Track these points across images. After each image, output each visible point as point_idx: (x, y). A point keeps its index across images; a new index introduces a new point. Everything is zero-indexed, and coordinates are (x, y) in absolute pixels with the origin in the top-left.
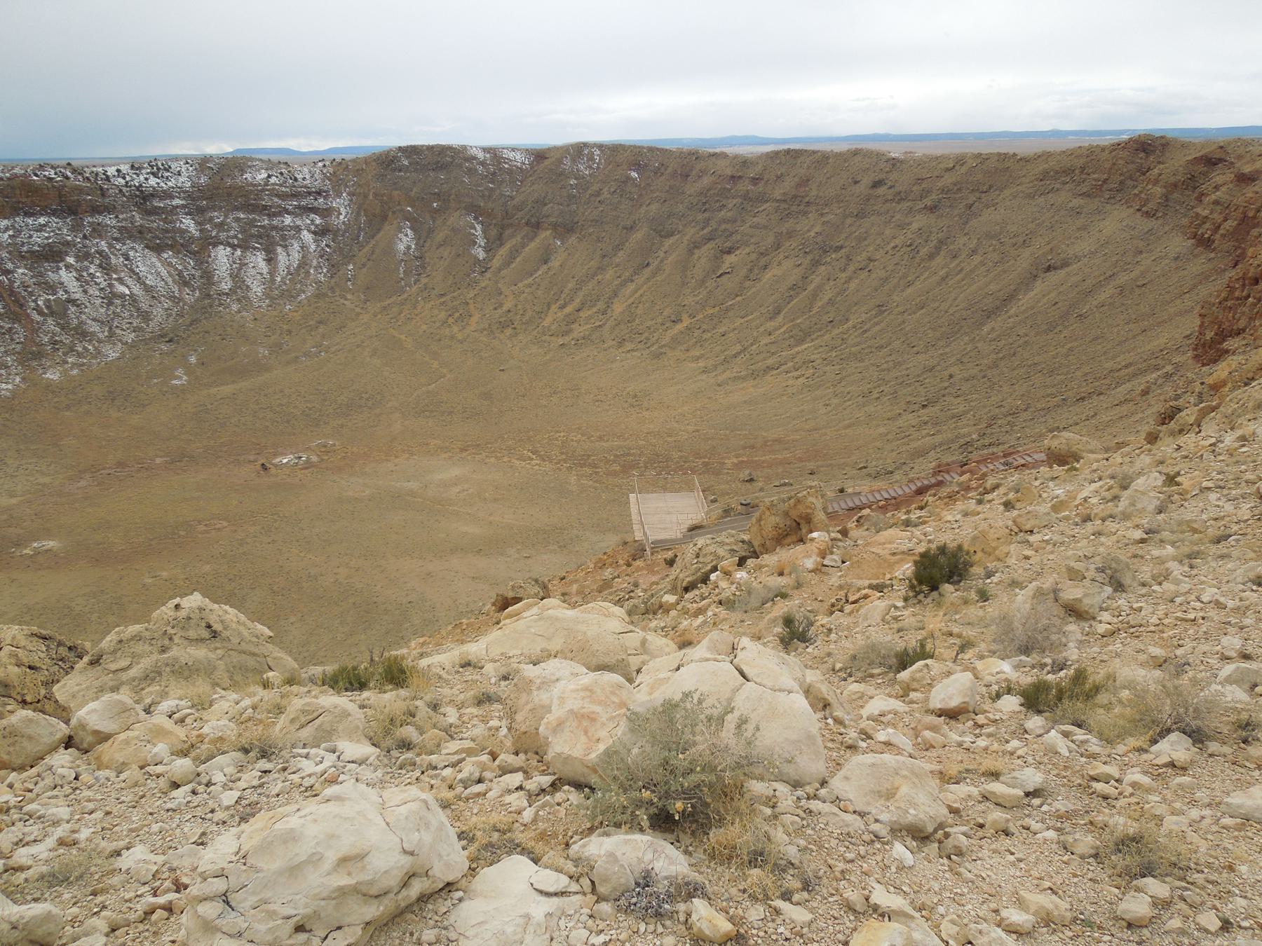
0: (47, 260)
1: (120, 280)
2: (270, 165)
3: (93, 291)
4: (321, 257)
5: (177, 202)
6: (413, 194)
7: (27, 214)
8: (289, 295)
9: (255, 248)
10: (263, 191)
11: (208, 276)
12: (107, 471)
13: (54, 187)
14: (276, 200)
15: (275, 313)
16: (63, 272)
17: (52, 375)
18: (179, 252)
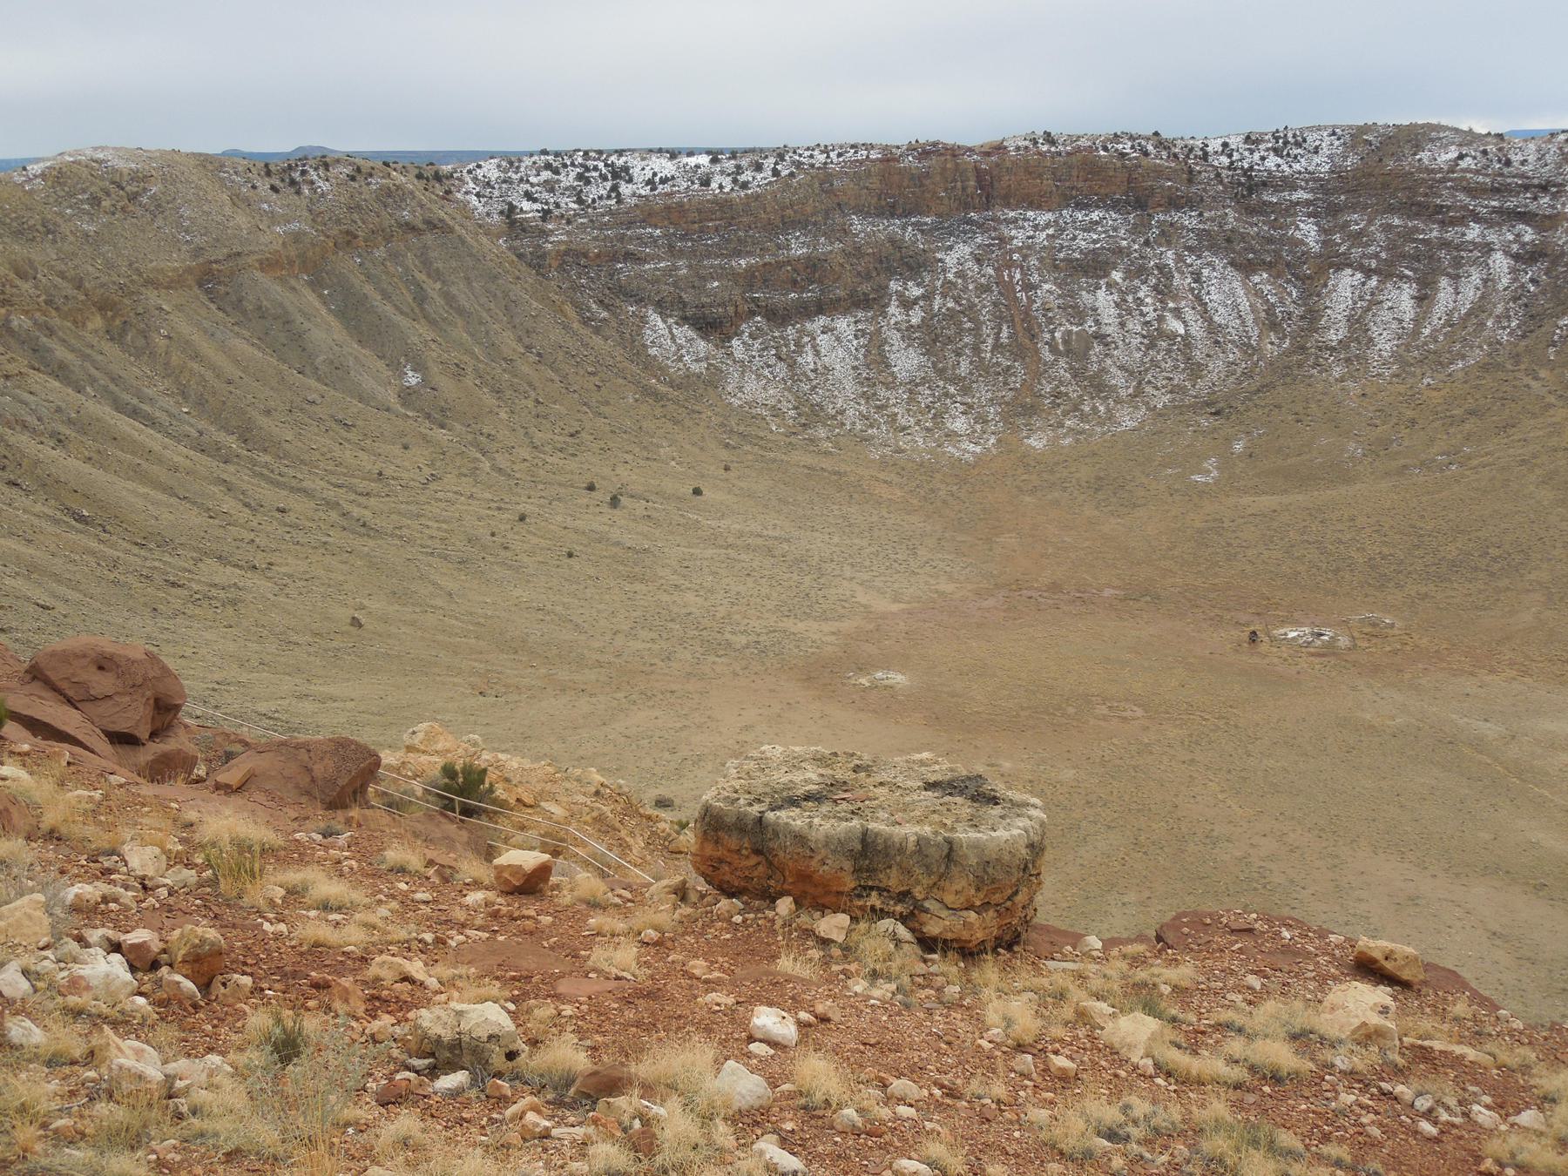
0: (1086, 274)
1: (1177, 313)
2: (1470, 138)
3: (1134, 325)
4: (1515, 299)
7: (1080, 206)
8: (1435, 360)
9: (1402, 277)
10: (1443, 180)
11: (1313, 317)
12: (1029, 593)
13: (1124, 166)
14: (1461, 196)
15: (1402, 389)
16: (1101, 293)
17: (1037, 442)
18: (1278, 276)
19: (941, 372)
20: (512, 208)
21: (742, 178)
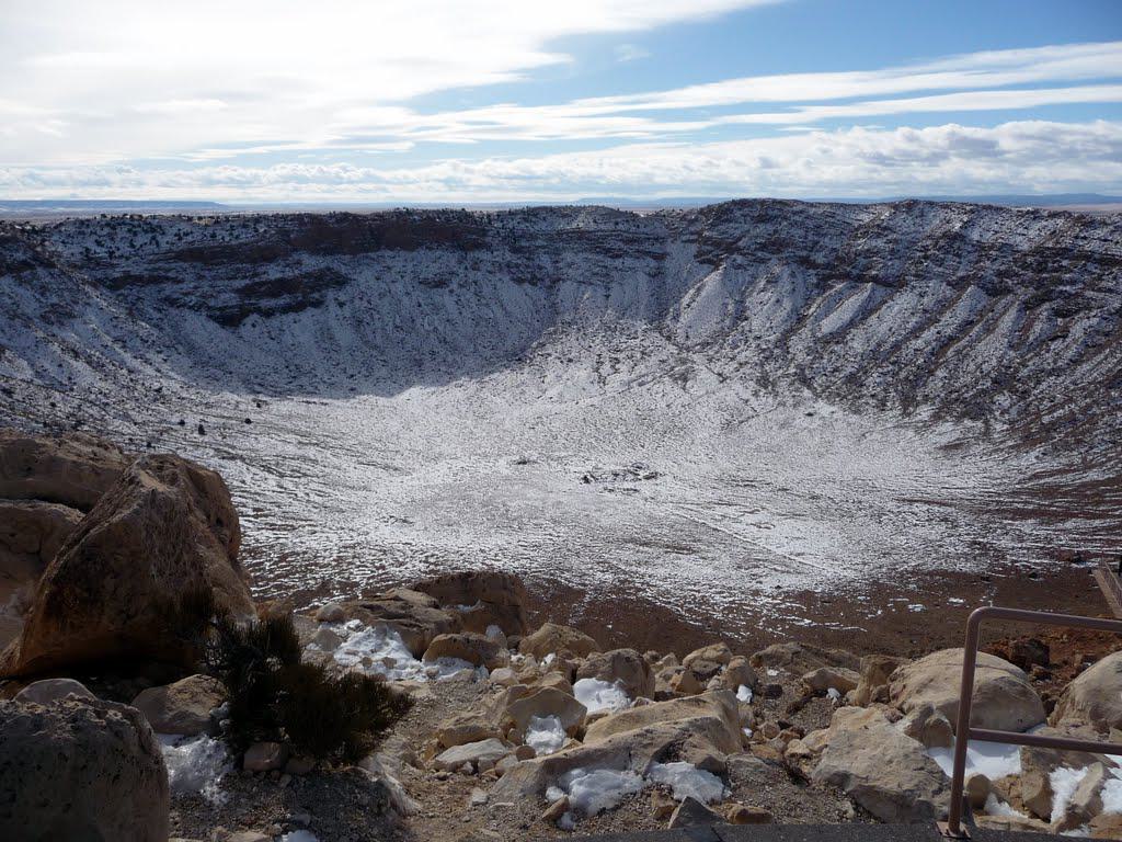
5: (539, 242)
6: (740, 243)
19: (366, 343)
20: (87, 249)
21: (236, 233)
